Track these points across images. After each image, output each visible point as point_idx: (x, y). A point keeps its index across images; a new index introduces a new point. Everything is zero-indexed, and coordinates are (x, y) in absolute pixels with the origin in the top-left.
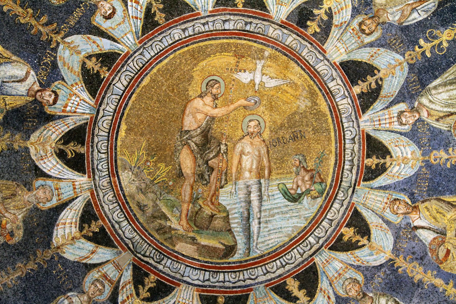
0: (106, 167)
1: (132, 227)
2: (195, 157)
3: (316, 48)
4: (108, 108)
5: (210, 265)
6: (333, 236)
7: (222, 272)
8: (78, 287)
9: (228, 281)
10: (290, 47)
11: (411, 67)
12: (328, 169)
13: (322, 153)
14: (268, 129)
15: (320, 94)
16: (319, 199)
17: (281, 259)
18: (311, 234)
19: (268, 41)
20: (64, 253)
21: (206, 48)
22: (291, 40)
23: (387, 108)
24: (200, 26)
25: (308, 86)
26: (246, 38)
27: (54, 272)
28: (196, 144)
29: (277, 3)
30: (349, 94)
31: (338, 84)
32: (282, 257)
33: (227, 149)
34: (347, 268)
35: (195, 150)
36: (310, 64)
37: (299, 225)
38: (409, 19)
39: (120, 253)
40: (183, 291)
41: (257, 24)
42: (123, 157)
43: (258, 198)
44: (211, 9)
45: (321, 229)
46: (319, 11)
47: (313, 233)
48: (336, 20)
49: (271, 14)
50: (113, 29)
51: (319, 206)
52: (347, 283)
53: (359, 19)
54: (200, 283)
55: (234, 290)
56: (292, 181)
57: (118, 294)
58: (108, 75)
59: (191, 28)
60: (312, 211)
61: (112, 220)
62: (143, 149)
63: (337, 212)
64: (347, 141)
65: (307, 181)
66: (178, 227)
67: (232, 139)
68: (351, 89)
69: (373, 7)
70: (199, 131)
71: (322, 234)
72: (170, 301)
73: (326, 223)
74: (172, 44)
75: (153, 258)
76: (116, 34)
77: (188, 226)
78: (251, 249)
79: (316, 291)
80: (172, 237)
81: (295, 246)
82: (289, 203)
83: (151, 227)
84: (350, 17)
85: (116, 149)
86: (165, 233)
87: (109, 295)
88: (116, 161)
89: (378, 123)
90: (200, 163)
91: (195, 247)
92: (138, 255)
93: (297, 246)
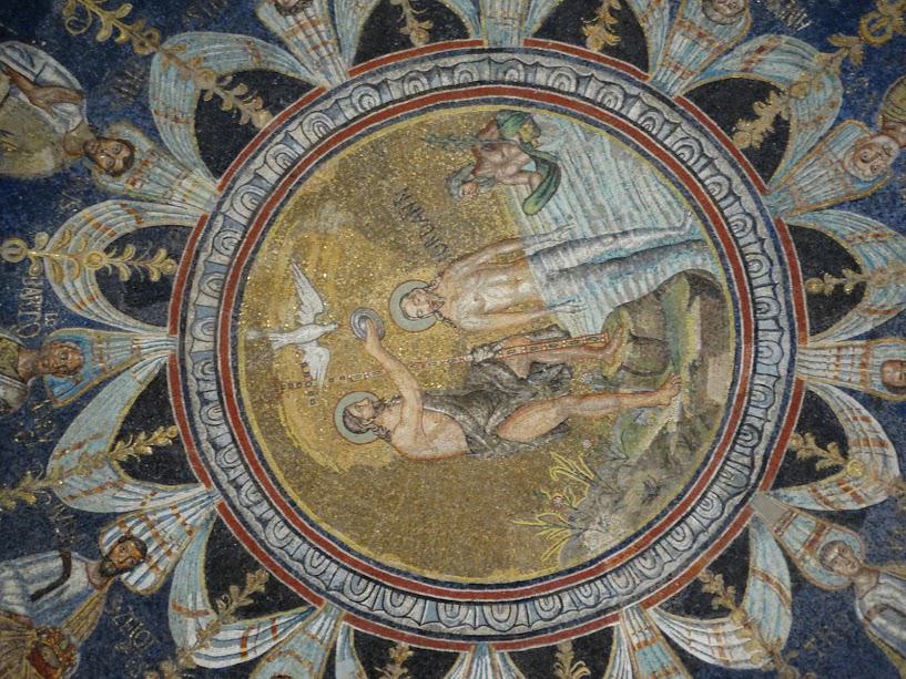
0: (588, 589)
1: (698, 504)
2: (517, 409)
3: (204, 240)
4: (469, 621)
5: (742, 321)
6: (613, 68)
7: (752, 294)
8: (843, 599)
9: (770, 276)
10: (221, 293)
11: (168, 30)
12: (463, 118)
13: (430, 142)
14: (414, 275)
15: (300, 192)
16: (534, 118)
17: (696, 169)
18: (622, 116)
19: (224, 345)
20: (779, 639)
21: (284, 463)
22: (204, 297)
23: (280, 43)
24: (244, 494)
25: (291, 222)
26: (234, 391)
27: (821, 655)
28: (490, 414)
29: (137, 360)
30: (278, 132)
31: (265, 162)
32: (689, 168)
33: (482, 347)
34: (681, 22)
35: (503, 414)
36: (243, 237)
37: (607, 147)
38: (62, 82)
39: (756, 519)
40: (812, 373)
41: (198, 380)
42: (558, 558)
43: (570, 250)
44: (203, 488)
45: (603, 98)
46: (122, 269)
47: (617, 113)
48: (127, 225)
49: (166, 360)
50: (312, 668)
51: (553, 115)
52: (717, 16)
53: (105, 181)
54: (787, 336)
55: (786, 260)
56: (512, 187)
57: (844, 512)
58: (403, 644)
59: (255, 509)
60: (567, 128)
61: (693, 551)
62: (531, 521)
63: (556, 73)
64: (386, 98)
65: (503, 155)
66: (676, 405)
67: (458, 343)
68: (265, 134)
69: (67, 166)
70: (460, 417)
71: (616, 91)
72: (838, 398)
73: (589, 90)
74: (300, 536)
75: (753, 448)
76: (318, 657)
77: (668, 386)
78: (687, 238)
79: (749, 82)
80: (700, 416)
81: (659, 146)
82: (564, 180)
83: (690, 465)
84: (109, 202)
85: (546, 578)
86: (694, 432)
87: (849, 531)
88: (571, 571)
89: (322, 49)
90: (528, 393)
91: (711, 361)
92: (753, 481)
93: (657, 141)
